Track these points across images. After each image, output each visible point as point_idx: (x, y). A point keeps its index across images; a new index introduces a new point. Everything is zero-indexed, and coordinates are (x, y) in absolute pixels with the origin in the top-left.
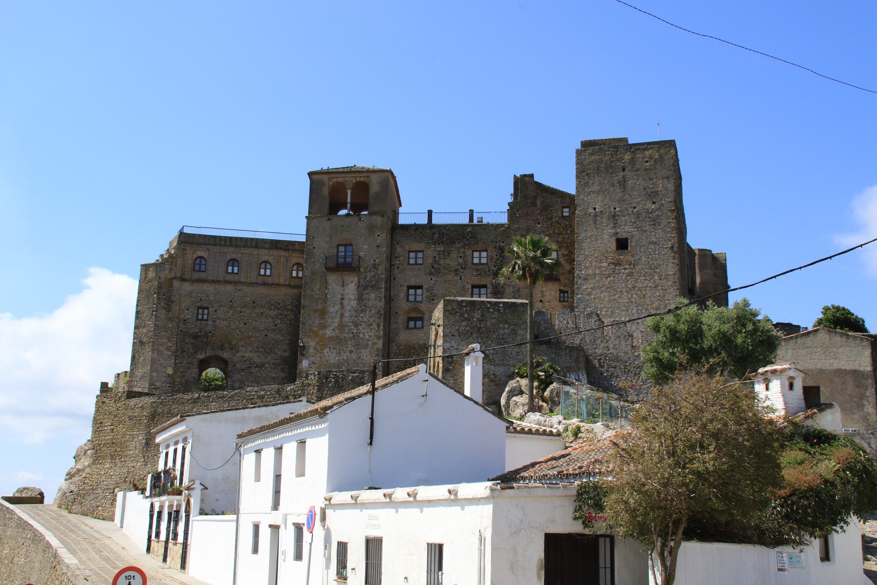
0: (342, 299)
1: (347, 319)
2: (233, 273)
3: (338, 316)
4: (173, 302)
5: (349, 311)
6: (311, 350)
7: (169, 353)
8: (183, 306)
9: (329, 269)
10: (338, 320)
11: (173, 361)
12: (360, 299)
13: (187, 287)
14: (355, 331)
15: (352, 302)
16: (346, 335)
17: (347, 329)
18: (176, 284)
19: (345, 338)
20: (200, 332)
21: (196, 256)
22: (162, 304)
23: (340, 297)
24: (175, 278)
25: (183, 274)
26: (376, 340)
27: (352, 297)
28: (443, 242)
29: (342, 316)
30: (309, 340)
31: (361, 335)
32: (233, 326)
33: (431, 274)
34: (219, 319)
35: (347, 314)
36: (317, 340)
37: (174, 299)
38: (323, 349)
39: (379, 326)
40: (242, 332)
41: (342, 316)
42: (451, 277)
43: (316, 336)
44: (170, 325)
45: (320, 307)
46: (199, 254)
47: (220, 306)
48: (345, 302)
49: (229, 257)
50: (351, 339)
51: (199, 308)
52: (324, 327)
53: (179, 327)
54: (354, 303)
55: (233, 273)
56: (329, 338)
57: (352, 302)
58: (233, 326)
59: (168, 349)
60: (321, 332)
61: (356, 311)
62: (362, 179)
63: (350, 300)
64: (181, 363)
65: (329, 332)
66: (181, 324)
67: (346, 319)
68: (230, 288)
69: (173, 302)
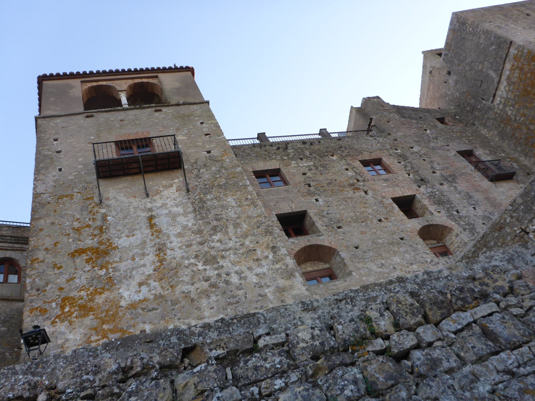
0: (151, 218)
1: (179, 253)
3: (150, 250)
5: (179, 235)
9: (107, 170)
10: (151, 258)
12: (200, 209)
14: (212, 273)
15: (181, 219)
16: (186, 288)
17: (185, 275)
19: (186, 295)
23: (144, 214)
26: (282, 282)
27: (180, 210)
28: (307, 157)
29: (161, 249)
31: (235, 279)
33: (310, 194)
35: (175, 242)
36: (89, 321)
39: (274, 249)
41: (161, 249)
42: (350, 193)
43: (85, 310)
48: (162, 222)
50: (206, 294)
52: (110, 283)
54: (189, 221)
56: (133, 306)
57: (181, 219)
60: (100, 299)
61: (199, 232)
62: (144, 80)
63: (174, 217)
65: (128, 293)
67: (176, 251)
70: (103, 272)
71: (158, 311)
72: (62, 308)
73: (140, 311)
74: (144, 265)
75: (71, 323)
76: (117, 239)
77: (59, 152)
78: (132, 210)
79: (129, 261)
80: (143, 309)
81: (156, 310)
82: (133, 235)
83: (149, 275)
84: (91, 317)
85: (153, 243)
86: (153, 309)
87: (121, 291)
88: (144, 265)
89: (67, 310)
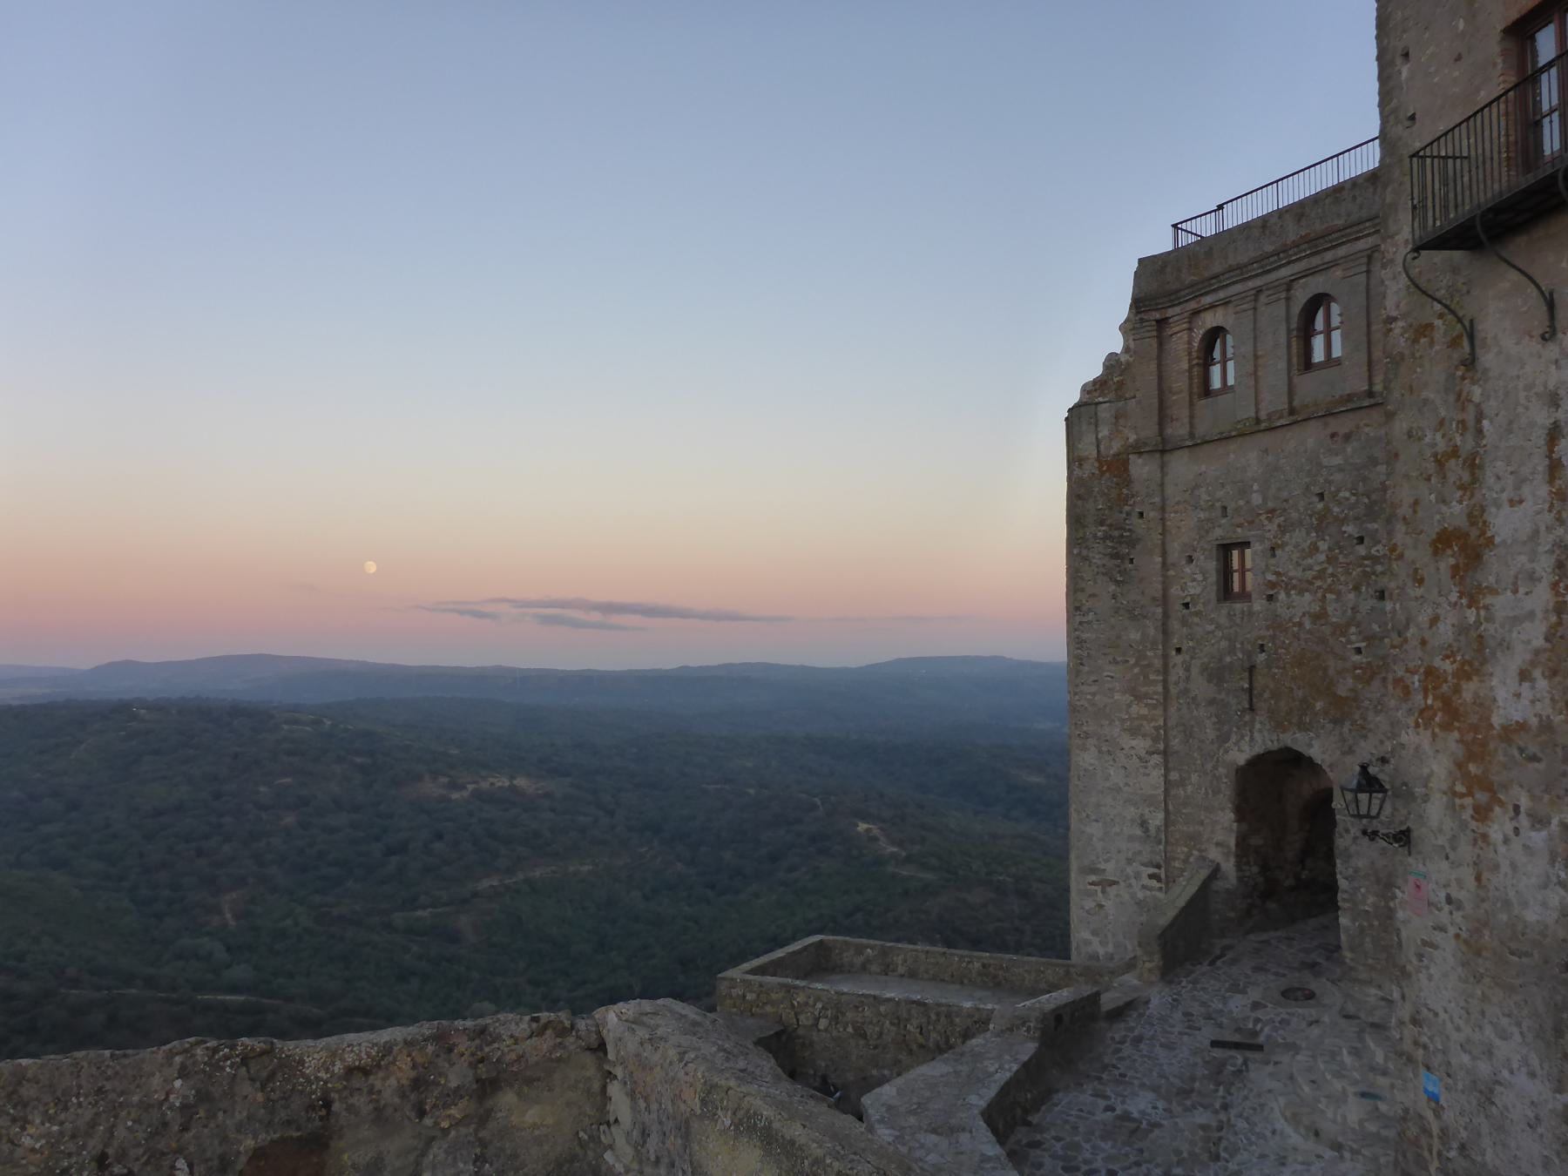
2: (1330, 361)
4: (1132, 542)
6: (1435, 809)
7: (1141, 744)
8: (1175, 548)
11: (1156, 775)
13: (1182, 468)
18: (1141, 469)
20: (1232, 651)
21: (1199, 334)
22: (1097, 559)
24: (1138, 449)
25: (1163, 419)
30: (1424, 739)
32: (1335, 614)
34: (1288, 588)
37: (1138, 525)
38: (1482, 813)
40: (1370, 639)
44: (1135, 636)
45: (1456, 512)
46: (1210, 320)
47: (1283, 529)
49: (1301, 296)
51: (1225, 549)
53: (1166, 632)
55: (1330, 361)
58: (1335, 614)
59: (1134, 732)
64: (1182, 783)
66: (1175, 625)
68: (1311, 437)
69: (1132, 542)
70: (1471, 615)
71: (1541, 766)
72: (1426, 698)
73: (1516, 752)
74: (1531, 615)
75: (1434, 735)
76: (1493, 510)
77: (1412, 118)
78: (1522, 395)
79: (1509, 593)
80: (1521, 750)
81: (1539, 760)
82: (1521, 502)
83: (1537, 652)
84: (1456, 735)
85: (1551, 538)
86: (1534, 758)
87: (1495, 682)
88: (1531, 615)
89: (1429, 702)
